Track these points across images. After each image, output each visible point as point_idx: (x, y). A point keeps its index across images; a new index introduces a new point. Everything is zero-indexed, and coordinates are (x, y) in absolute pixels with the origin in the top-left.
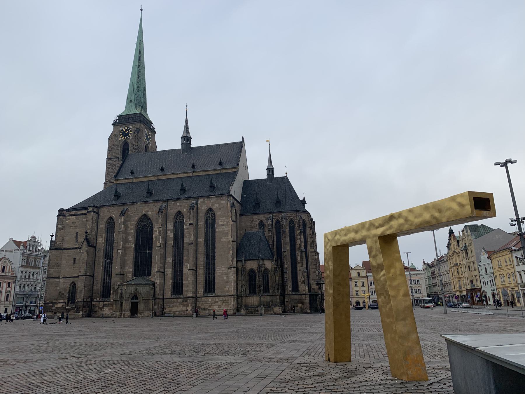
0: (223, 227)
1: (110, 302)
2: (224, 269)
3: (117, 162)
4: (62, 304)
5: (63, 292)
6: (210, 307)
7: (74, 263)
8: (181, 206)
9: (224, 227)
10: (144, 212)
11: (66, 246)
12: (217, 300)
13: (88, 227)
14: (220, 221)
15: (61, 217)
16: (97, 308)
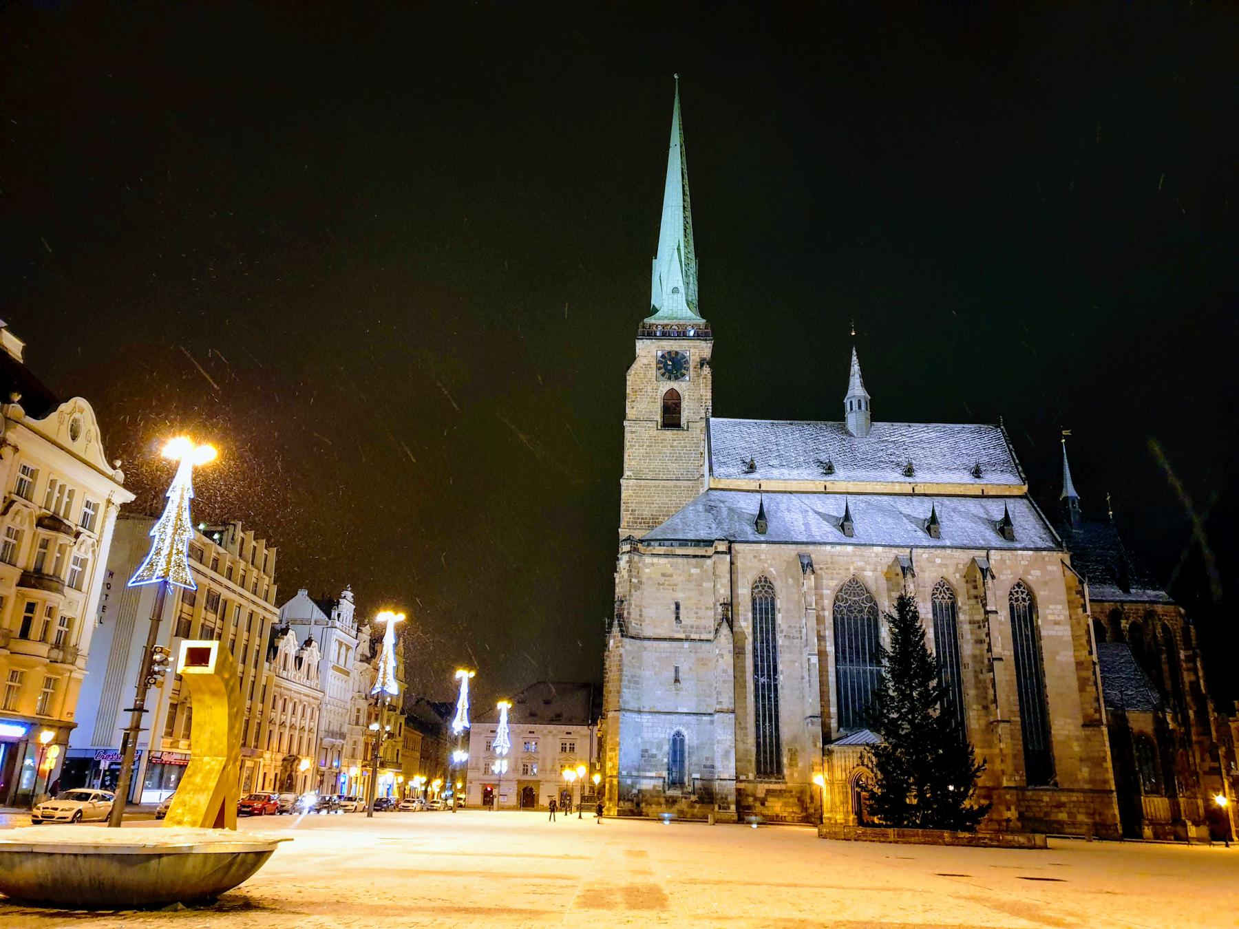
0: (1057, 627)
1: (783, 787)
2: (1072, 727)
3: (654, 432)
4: (653, 782)
5: (654, 751)
6: (1047, 814)
7: (677, 681)
8: (946, 565)
9: (1061, 628)
10: (852, 571)
11: (648, 632)
12: (1063, 799)
13: (722, 591)
14: (1048, 611)
15: (636, 558)
16: (751, 799)
